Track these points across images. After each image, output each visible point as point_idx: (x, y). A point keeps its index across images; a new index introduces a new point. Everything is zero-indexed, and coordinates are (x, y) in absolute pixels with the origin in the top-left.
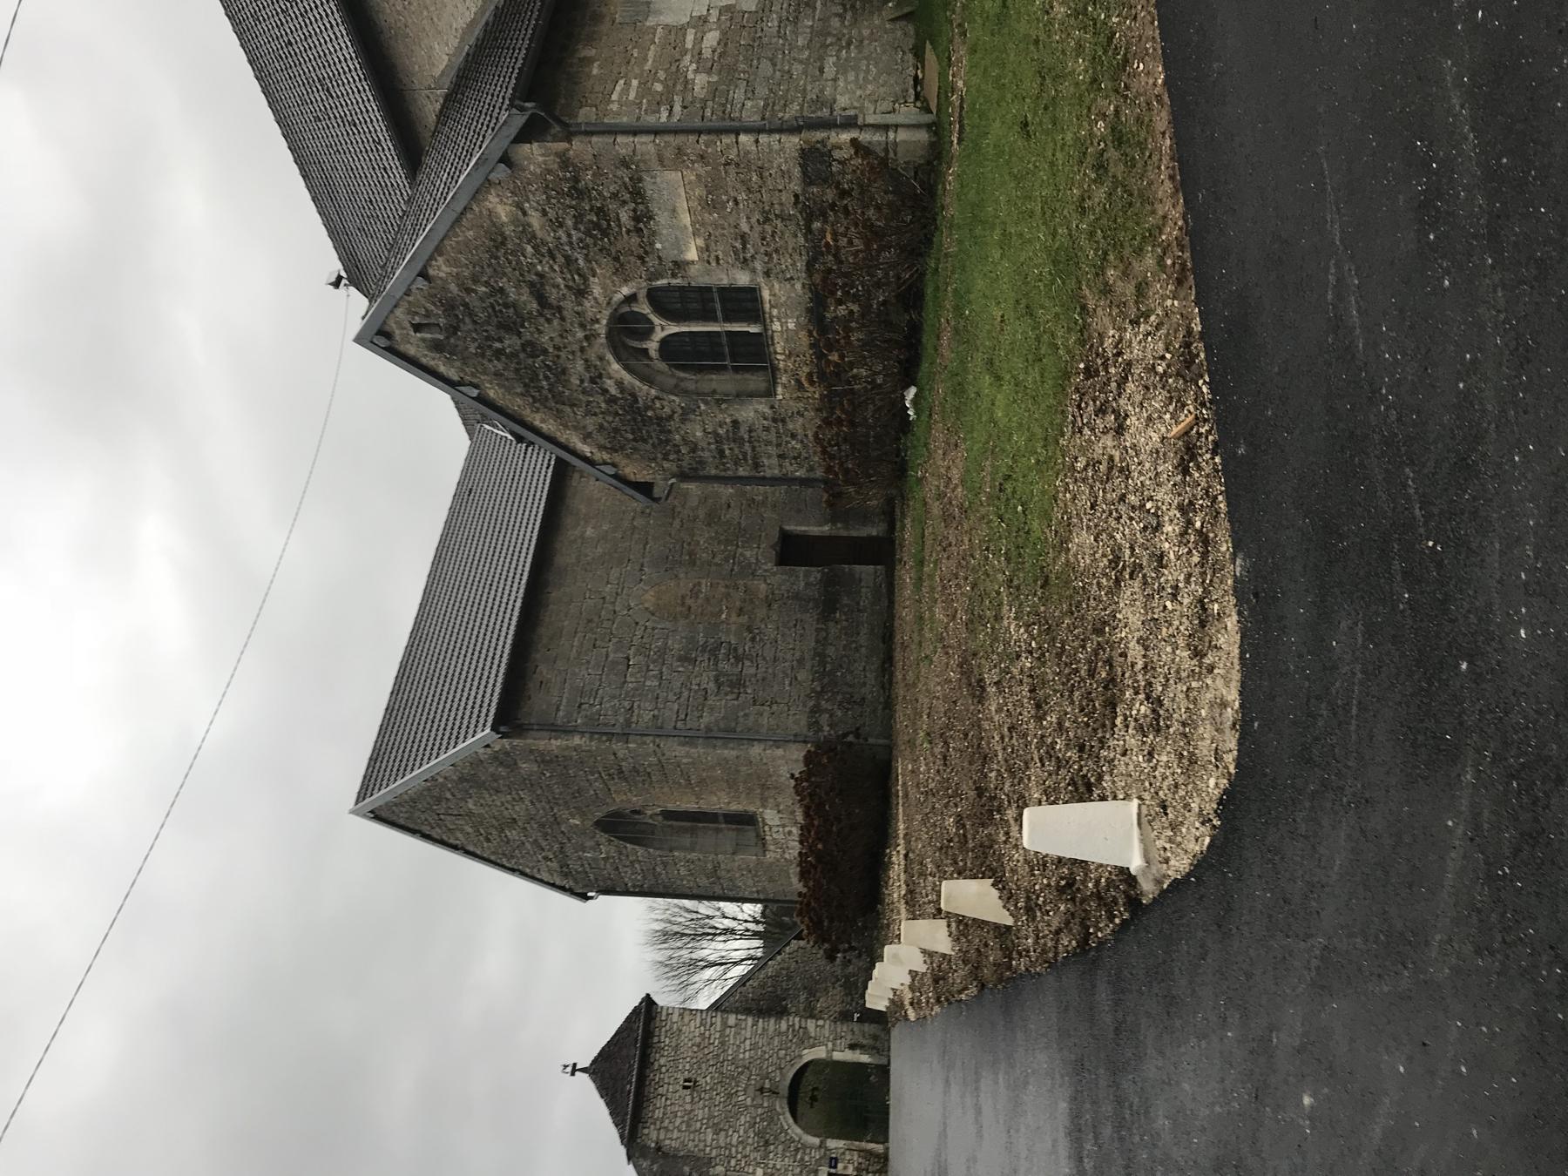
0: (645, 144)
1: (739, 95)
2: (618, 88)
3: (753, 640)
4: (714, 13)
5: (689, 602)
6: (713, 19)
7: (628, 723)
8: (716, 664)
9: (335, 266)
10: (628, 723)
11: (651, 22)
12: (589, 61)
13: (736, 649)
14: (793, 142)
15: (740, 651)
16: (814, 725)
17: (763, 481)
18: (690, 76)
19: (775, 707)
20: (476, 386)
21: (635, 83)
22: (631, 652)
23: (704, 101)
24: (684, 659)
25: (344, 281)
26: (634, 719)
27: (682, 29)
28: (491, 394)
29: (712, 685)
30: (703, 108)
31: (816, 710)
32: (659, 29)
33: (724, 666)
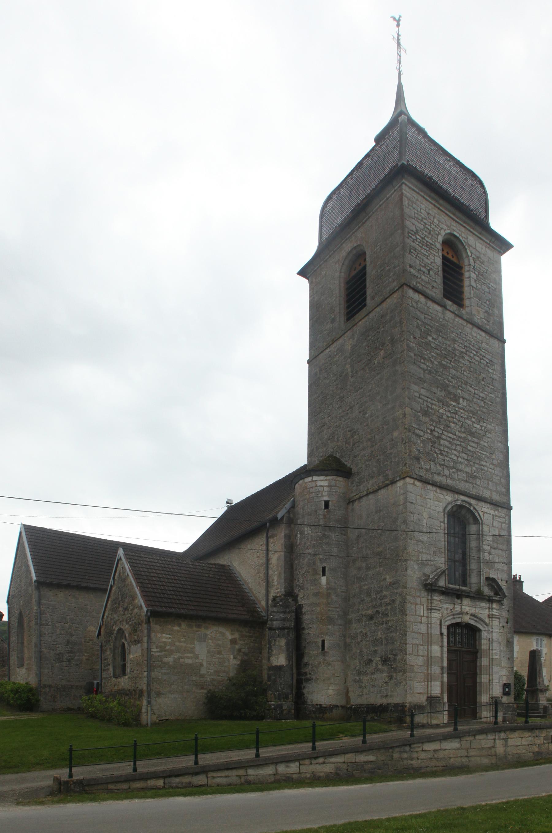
0: (145, 645)
1: (164, 670)
2: (167, 636)
3: (77, 665)
4: (200, 661)
5: (91, 642)
6: (197, 661)
7: (43, 625)
8: (67, 653)
9: (236, 501)
10: (43, 625)
11: (196, 642)
12: (180, 625)
13: (72, 659)
14: (145, 688)
15: (72, 661)
16: (45, 686)
17: (101, 673)
18: (172, 656)
19: (51, 673)
20: (114, 583)
21: (170, 640)
22: (70, 624)
23: (161, 661)
24: (68, 642)
25: (230, 505)
26: (44, 627)
27: (193, 652)
28: (113, 589)
29: (58, 651)
30: (158, 661)
31: (50, 686)
32: (193, 645)
33: (66, 656)
